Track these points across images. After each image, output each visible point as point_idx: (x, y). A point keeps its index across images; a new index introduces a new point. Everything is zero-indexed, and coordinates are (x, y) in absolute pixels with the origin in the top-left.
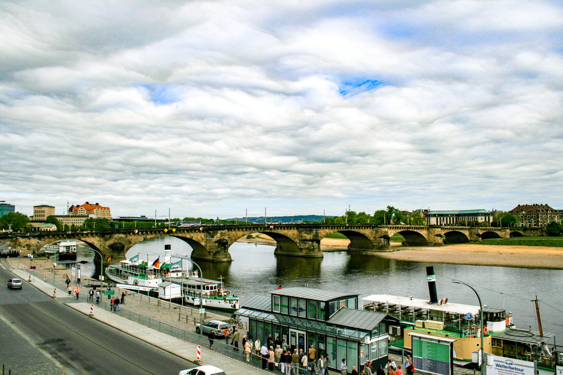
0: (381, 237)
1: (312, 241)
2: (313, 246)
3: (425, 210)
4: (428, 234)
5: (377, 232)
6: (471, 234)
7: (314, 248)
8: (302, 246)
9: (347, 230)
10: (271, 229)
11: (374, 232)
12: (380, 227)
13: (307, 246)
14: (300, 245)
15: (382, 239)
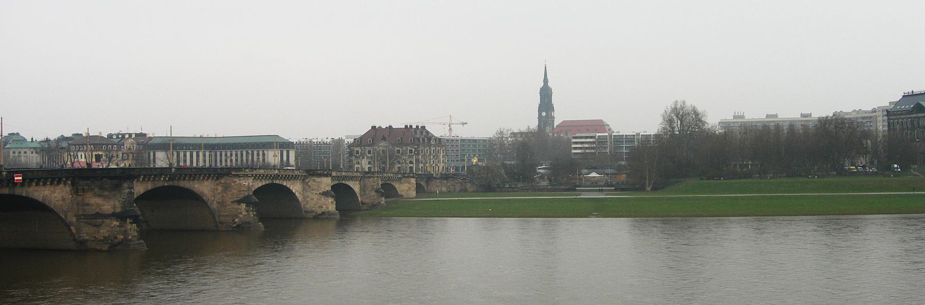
0: (239, 202)
1: (121, 217)
2: (125, 233)
3: (137, 135)
4: (304, 189)
5: (226, 188)
6: (363, 189)
7: (126, 239)
8: (86, 232)
9: (171, 183)
10: (15, 184)
11: (220, 188)
12: (238, 176)
13: (104, 232)
14: (78, 230)
15: (243, 206)
